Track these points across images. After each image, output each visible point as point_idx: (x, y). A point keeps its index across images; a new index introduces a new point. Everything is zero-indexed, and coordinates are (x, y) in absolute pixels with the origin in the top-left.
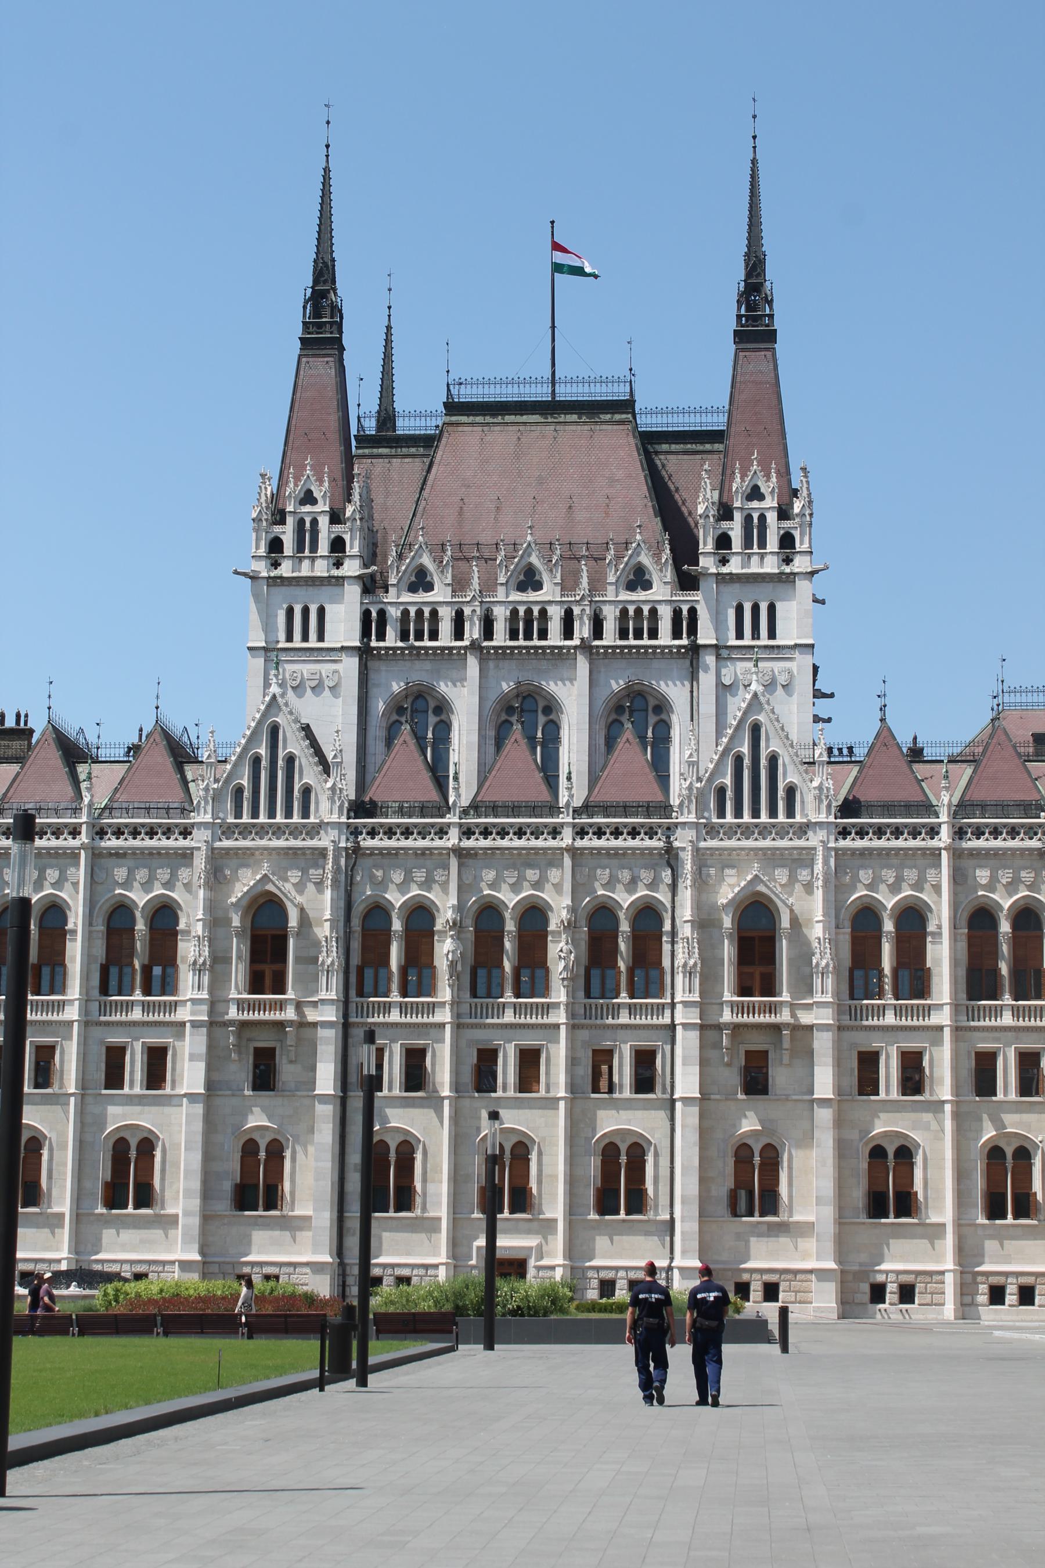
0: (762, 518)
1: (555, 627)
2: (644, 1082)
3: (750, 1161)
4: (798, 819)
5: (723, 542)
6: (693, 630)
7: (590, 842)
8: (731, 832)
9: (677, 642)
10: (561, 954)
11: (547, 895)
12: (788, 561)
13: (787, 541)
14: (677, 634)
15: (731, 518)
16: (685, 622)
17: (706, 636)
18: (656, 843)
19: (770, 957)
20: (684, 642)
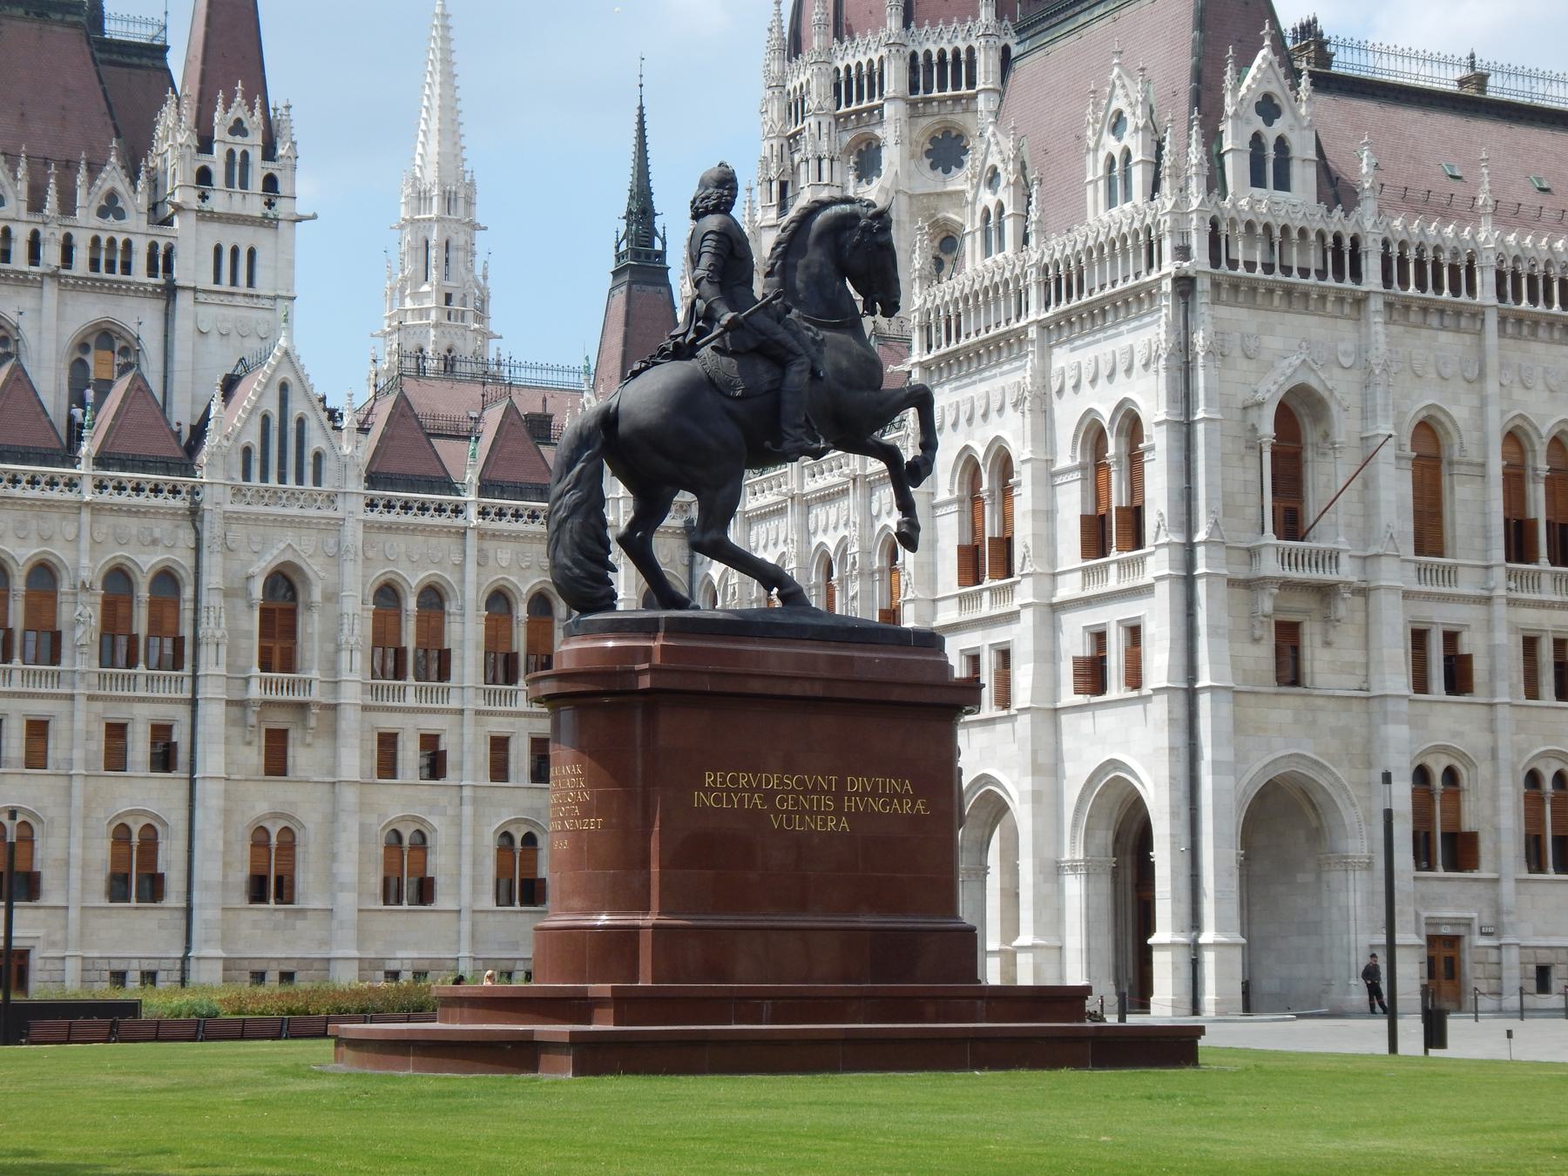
0: (245, 154)
1: (20, 250)
2: (164, 758)
3: (267, 845)
4: (326, 487)
5: (204, 176)
6: (168, 268)
7: (107, 497)
8: (260, 495)
9: (153, 280)
10: (81, 618)
11: (60, 552)
12: (270, 204)
13: (270, 183)
14: (152, 270)
15: (210, 152)
16: (162, 261)
17: (180, 275)
18: (179, 503)
19: (291, 632)
20: (160, 280)
